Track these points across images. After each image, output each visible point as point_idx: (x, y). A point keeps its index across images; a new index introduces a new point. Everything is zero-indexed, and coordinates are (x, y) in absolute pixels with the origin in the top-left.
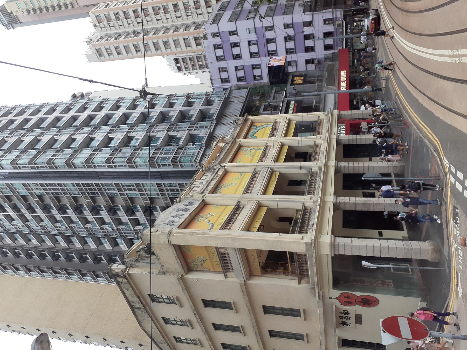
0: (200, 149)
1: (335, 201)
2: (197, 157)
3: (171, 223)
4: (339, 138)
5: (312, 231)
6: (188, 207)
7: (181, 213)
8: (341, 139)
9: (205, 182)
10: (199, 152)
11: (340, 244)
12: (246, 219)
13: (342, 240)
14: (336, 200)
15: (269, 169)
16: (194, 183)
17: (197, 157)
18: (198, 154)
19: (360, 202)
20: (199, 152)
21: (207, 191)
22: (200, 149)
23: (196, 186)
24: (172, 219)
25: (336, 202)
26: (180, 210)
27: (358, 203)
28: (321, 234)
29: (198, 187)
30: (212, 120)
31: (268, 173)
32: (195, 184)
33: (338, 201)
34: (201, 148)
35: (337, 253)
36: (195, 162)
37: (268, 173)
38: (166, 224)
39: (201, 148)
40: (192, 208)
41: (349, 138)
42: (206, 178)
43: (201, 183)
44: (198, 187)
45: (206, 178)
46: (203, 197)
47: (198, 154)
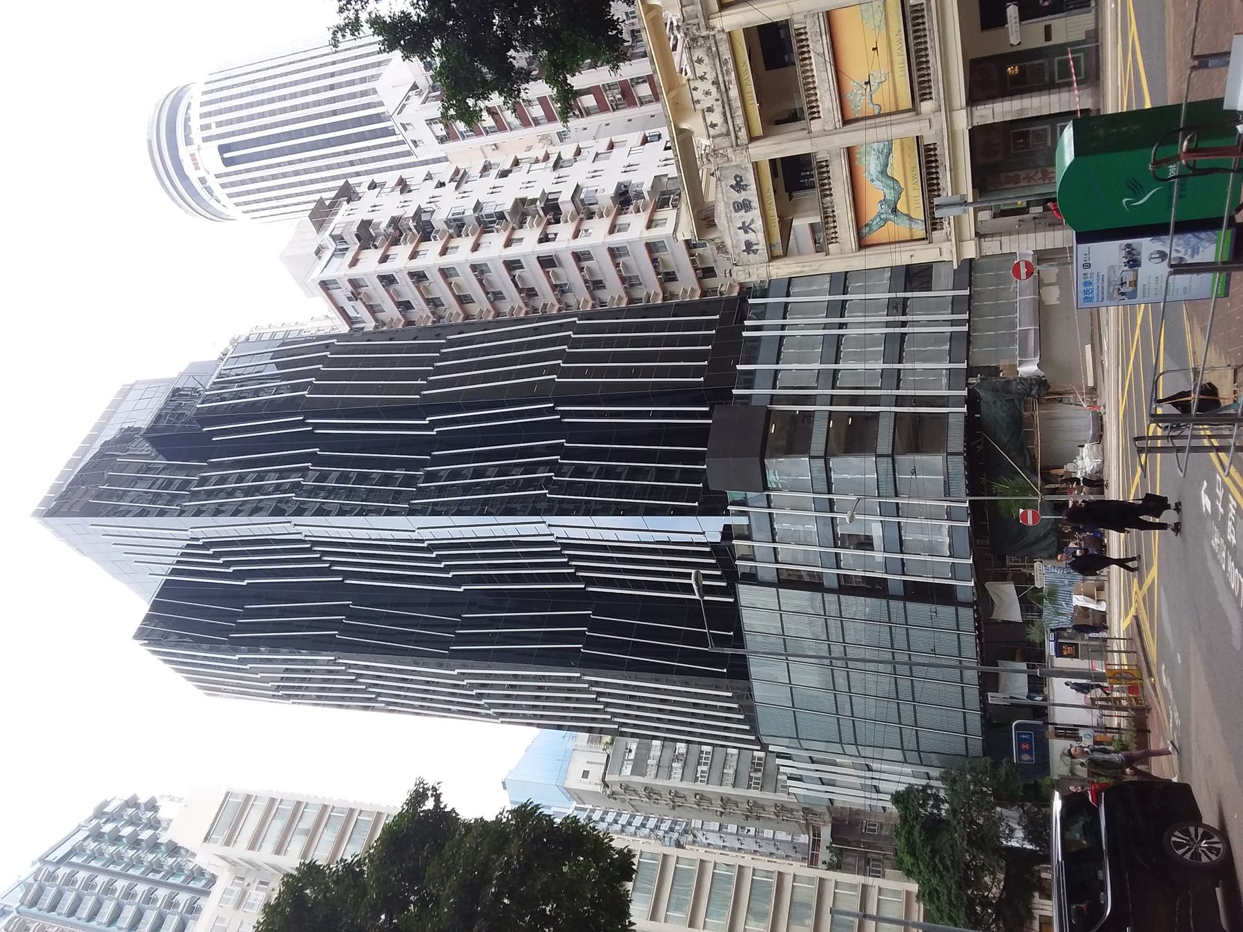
3: (749, 247)
5: (949, 224)
6: (743, 196)
7: (747, 216)
9: (713, 90)
12: (850, 216)
15: (821, 14)
16: (695, 99)
21: (740, 129)
24: (743, 237)
29: (710, 110)
31: (824, 37)
33: (975, 124)
37: (824, 37)
40: (751, 194)
42: (705, 73)
43: (707, 93)
44: (710, 110)
45: (705, 73)
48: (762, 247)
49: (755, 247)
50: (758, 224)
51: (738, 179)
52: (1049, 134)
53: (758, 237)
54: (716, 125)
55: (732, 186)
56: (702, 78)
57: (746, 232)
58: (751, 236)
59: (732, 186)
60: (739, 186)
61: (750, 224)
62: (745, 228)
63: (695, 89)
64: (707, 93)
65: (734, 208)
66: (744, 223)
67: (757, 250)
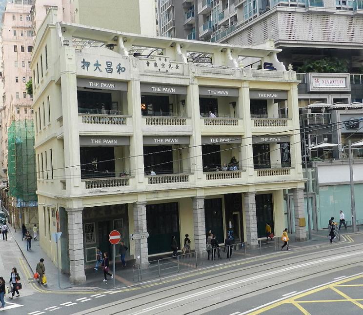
0: (300, 6)
1: (137, 203)
2: (287, 5)
3: (86, 64)
4: (249, 195)
6: (115, 70)
7: (104, 67)
8: (248, 197)
9: (164, 70)
10: (296, 6)
11: (73, 216)
13: (78, 217)
14: (139, 204)
17: (287, 5)
18: (292, 5)
19: (139, 224)
20: (296, 6)
22: (300, 6)
23: (158, 62)
24: (93, 62)
25: (137, 205)
26: (109, 65)
27: (138, 223)
28: (82, 200)
29: (156, 65)
30: (356, 8)
32: (160, 59)
34: (304, 6)
35: (68, 213)
36: (279, 5)
38: (84, 62)
39: (304, 6)
40: (115, 75)
41: (250, 206)
43: (163, 65)
44: (156, 65)
46: (133, 79)
47: (292, 5)
48: (85, 73)
49: (86, 67)
50: (98, 74)
51: (123, 69)
52: (92, 243)
53: (91, 72)
54: (148, 65)
55: (120, 64)
56: (170, 65)
57: (95, 65)
58: (92, 67)
59: (120, 64)
60: (120, 69)
61: (99, 69)
62: (97, 65)
63: (166, 60)
64: (163, 65)
65: (109, 62)
66: (100, 65)
67: (84, 69)
